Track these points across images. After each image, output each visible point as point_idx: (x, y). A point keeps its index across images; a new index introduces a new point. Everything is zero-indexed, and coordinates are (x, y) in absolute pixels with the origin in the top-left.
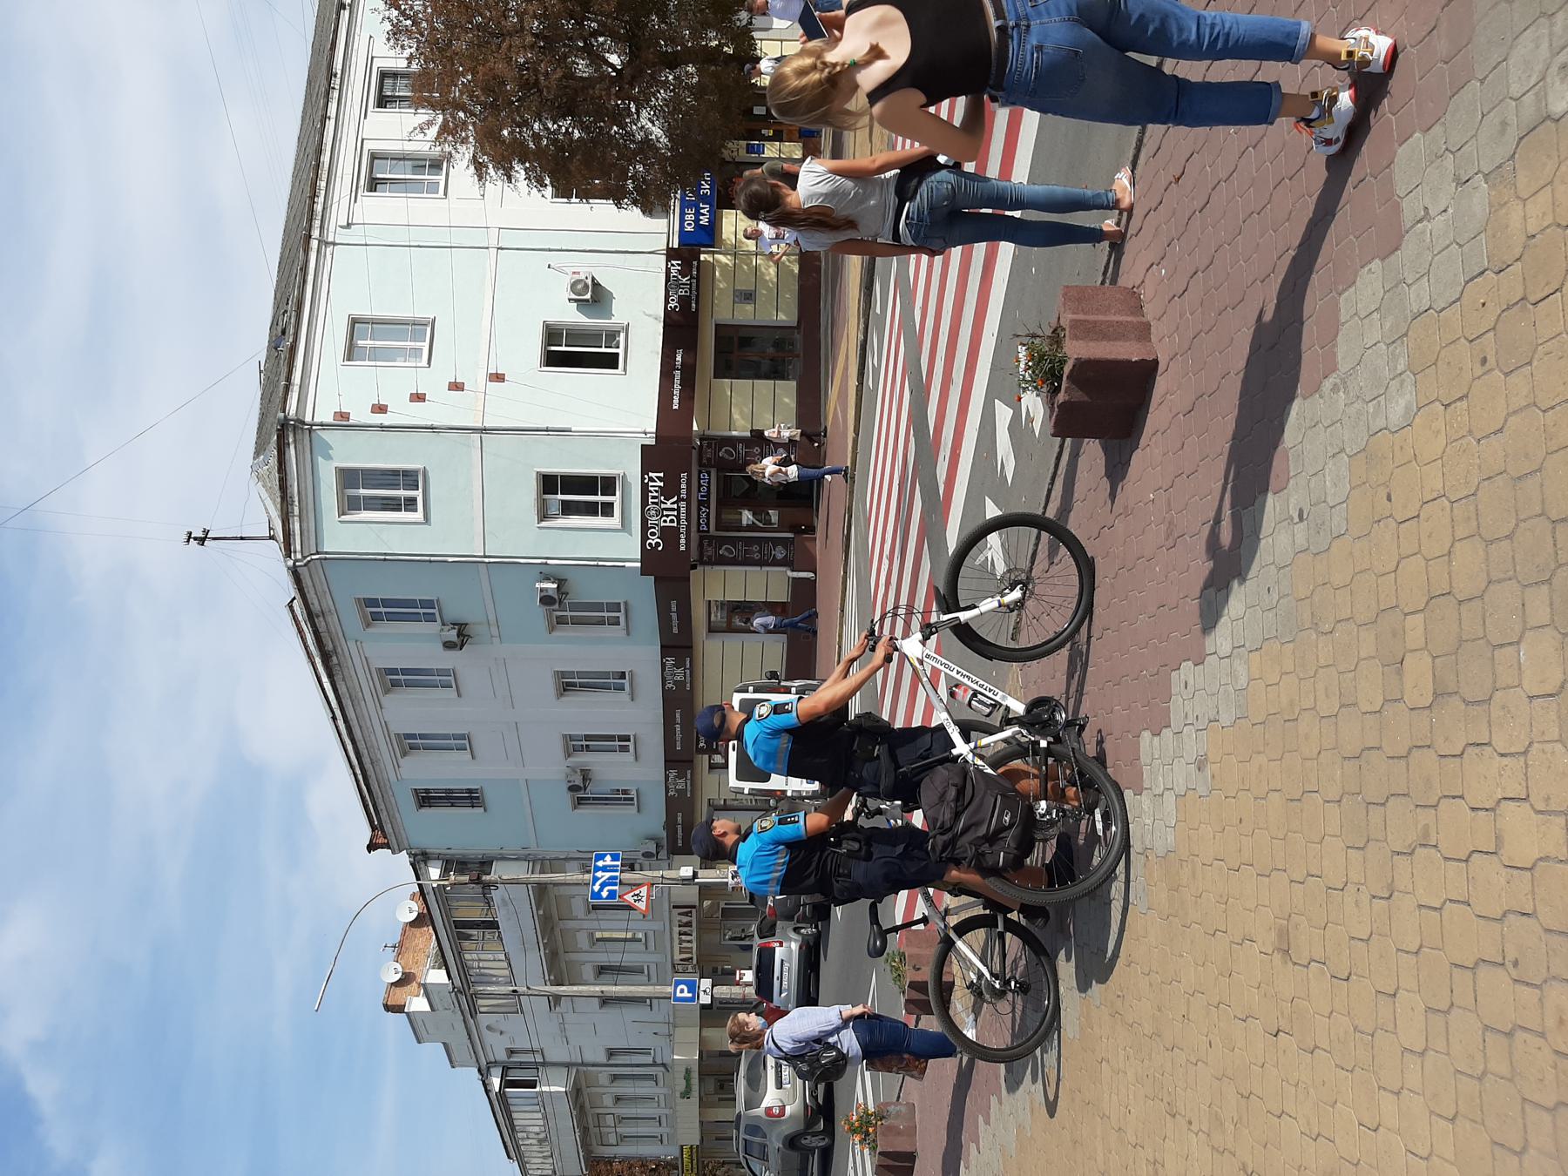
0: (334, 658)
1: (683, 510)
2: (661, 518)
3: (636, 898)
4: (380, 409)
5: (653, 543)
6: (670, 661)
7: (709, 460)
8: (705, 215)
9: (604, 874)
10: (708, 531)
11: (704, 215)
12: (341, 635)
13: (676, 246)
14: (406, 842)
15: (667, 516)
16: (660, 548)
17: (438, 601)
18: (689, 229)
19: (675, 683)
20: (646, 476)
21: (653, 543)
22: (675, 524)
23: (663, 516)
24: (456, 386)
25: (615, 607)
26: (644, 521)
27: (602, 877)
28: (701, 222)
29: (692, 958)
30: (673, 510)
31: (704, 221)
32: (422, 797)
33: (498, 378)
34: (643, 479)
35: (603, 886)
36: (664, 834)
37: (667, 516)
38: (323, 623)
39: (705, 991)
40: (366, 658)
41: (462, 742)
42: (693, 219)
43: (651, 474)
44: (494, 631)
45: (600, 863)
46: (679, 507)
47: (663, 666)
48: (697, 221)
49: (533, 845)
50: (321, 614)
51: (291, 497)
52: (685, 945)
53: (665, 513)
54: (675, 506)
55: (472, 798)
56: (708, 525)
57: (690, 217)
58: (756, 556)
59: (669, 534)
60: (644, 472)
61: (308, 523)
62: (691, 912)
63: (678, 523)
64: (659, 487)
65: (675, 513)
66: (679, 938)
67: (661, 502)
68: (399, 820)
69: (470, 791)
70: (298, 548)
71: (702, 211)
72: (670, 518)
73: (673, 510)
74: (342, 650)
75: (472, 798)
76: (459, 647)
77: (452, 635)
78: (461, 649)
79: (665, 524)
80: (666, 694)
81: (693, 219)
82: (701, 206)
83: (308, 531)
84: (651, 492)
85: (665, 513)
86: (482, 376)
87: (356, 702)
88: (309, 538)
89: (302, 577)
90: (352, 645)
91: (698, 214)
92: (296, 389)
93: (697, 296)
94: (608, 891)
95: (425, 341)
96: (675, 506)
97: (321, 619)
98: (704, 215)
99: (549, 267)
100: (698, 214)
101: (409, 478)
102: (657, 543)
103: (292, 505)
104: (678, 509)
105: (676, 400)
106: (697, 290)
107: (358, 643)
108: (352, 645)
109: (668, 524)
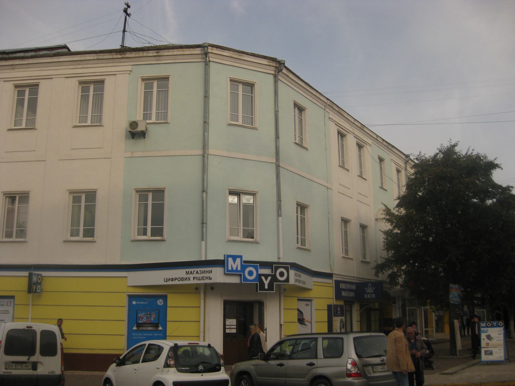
38: (151, 55)
40: (116, 74)
44: (141, 154)
50: (159, 54)
51: (242, 55)
74: (124, 62)
76: (132, 130)
77: (141, 128)
89: (191, 49)
90: (129, 68)
97: (155, 54)
107: (129, 72)
108: (129, 68)
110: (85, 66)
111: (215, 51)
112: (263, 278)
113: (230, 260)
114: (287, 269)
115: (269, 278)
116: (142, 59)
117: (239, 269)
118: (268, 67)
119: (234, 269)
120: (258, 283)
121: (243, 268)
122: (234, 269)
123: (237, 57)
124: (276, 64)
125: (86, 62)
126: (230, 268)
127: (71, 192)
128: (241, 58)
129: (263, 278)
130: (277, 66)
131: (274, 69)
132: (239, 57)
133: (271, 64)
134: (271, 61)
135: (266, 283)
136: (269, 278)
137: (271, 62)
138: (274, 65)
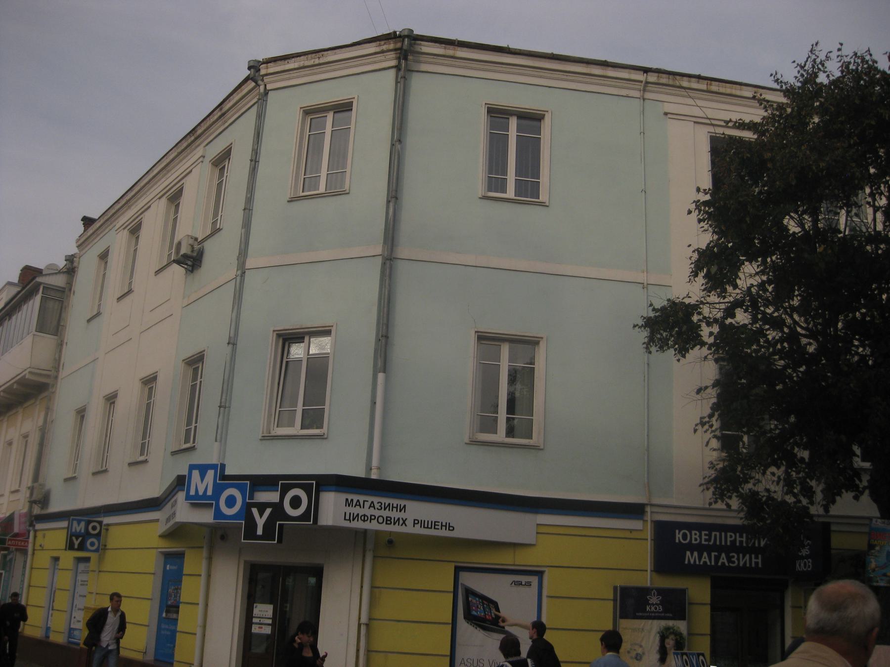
8: (700, 561)
11: (700, 559)
18: (679, 536)
28: (688, 553)
31: (691, 558)
42: (693, 542)
48: (691, 547)
57: (695, 537)
70: (271, 70)
71: (705, 554)
81: (693, 542)
82: (713, 554)
83: (289, 79)
91: (700, 549)
95: (515, 196)
111: (273, 68)
112: (255, 511)
113: (196, 474)
114: (307, 489)
115: (268, 511)
117: (210, 493)
118: (380, 57)
119: (201, 493)
120: (244, 522)
121: (218, 490)
122: (201, 493)
123: (314, 62)
124: (395, 43)
126: (192, 493)
128: (322, 61)
129: (255, 511)
130: (399, 45)
131: (394, 56)
132: (317, 61)
133: (385, 47)
134: (382, 42)
135: (260, 522)
136: (268, 511)
137: (385, 43)
138: (392, 46)
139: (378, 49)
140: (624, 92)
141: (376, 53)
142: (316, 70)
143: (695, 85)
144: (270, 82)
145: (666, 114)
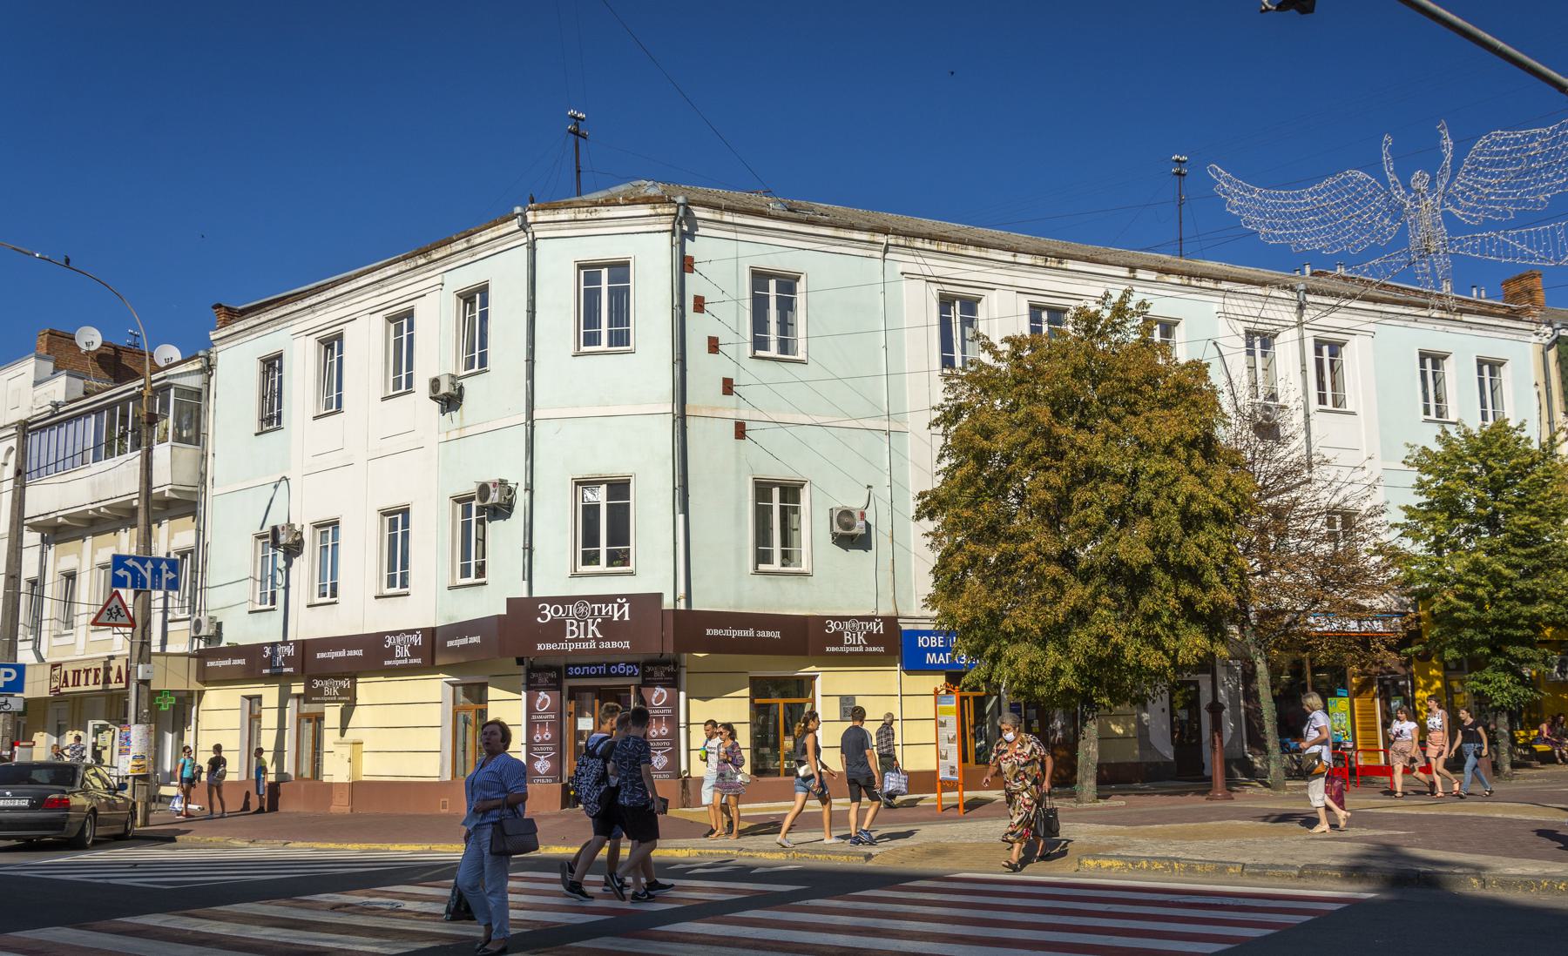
0: (423, 261)
1: (585, 646)
2: (575, 619)
3: (114, 610)
4: (700, 304)
5: (546, 612)
6: (417, 640)
7: (652, 674)
9: (149, 571)
10: (569, 677)
11: (938, 657)
12: (449, 267)
13: (904, 627)
14: (225, 346)
15: (578, 627)
16: (539, 619)
17: (486, 371)
18: (921, 641)
19: (393, 647)
20: (624, 600)
21: (546, 612)
22: (568, 637)
23: (578, 621)
24: (728, 387)
25: (481, 570)
26: (571, 600)
27: (146, 570)
28: (928, 655)
29: (67, 686)
30: (586, 633)
31: (931, 658)
32: (274, 364)
33: (740, 431)
34: (621, 596)
35: (133, 571)
36: (223, 644)
37: (578, 627)
38: (460, 248)
39: (6, 703)
40: (424, 295)
41: (333, 401)
43: (627, 605)
44: (455, 435)
45: (164, 566)
46: (588, 640)
47: (412, 632)
48: (931, 650)
49: (217, 491)
52: (83, 676)
53: (582, 624)
54: (590, 636)
55: (271, 418)
56: (574, 676)
58: (537, 737)
59: (556, 630)
60: (630, 597)
61: (569, 229)
62: (121, 681)
63: (570, 641)
64: (612, 616)
65: (582, 636)
66: (90, 670)
67: (595, 620)
68: (248, 338)
69: (279, 416)
70: (540, 219)
72: (576, 630)
73: (586, 633)
75: (271, 418)
77: (445, 388)
78: (431, 398)
79: (568, 624)
80: (381, 637)
84: (606, 607)
85: (582, 624)
86: (744, 415)
87: (377, 286)
88: (551, 230)
90: (438, 280)
91: (937, 651)
92: (717, 217)
93: (843, 654)
94: (126, 577)
96: (590, 636)
97: (465, 245)
98: (938, 657)
99: (869, 487)
100: (937, 651)
101: (620, 338)
102: (546, 616)
103: (587, 211)
104: (586, 640)
105: (716, 632)
106: (851, 653)
107: (440, 286)
109: (569, 628)
110: (391, 288)
116: (454, 258)
125: (389, 281)
127: (385, 513)
133: (659, 211)
139: (652, 212)
140: (868, 253)
141: (651, 216)
142: (588, 224)
143: (927, 246)
144: (538, 231)
145: (903, 274)
